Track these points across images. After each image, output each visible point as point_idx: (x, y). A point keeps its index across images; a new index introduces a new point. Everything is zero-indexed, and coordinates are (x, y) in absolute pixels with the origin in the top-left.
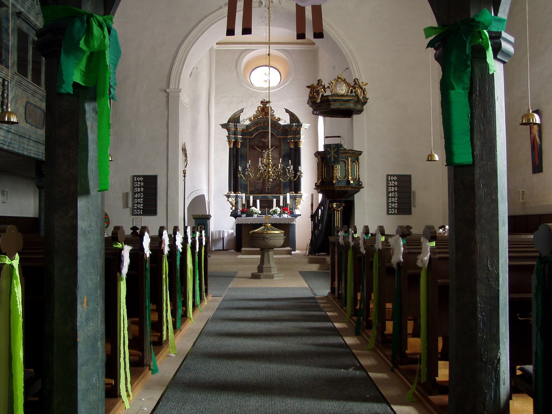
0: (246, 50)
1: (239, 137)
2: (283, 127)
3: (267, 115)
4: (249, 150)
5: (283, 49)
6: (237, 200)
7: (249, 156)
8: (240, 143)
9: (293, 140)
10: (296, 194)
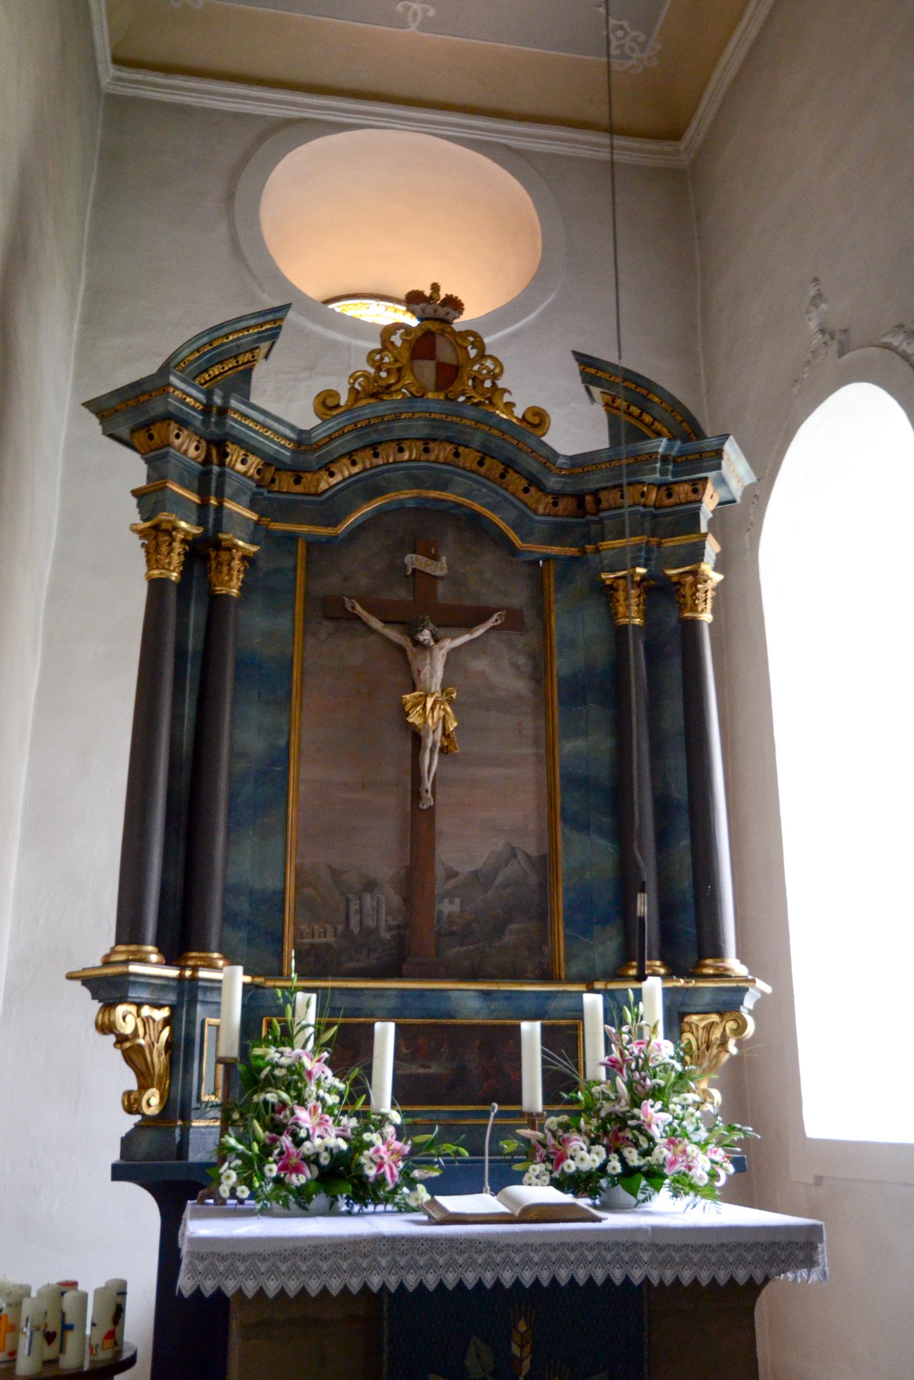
0: (289, 123)
1: (231, 512)
2: (571, 475)
3: (451, 382)
4: (306, 621)
5: (506, 146)
6: (191, 1022)
7: (303, 673)
8: (236, 563)
9: (641, 570)
10: (693, 983)
